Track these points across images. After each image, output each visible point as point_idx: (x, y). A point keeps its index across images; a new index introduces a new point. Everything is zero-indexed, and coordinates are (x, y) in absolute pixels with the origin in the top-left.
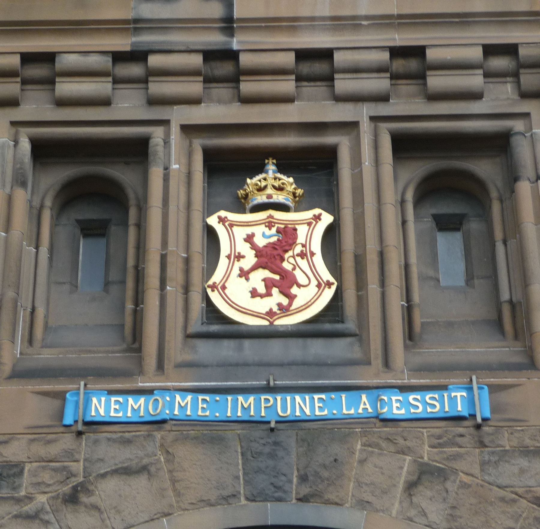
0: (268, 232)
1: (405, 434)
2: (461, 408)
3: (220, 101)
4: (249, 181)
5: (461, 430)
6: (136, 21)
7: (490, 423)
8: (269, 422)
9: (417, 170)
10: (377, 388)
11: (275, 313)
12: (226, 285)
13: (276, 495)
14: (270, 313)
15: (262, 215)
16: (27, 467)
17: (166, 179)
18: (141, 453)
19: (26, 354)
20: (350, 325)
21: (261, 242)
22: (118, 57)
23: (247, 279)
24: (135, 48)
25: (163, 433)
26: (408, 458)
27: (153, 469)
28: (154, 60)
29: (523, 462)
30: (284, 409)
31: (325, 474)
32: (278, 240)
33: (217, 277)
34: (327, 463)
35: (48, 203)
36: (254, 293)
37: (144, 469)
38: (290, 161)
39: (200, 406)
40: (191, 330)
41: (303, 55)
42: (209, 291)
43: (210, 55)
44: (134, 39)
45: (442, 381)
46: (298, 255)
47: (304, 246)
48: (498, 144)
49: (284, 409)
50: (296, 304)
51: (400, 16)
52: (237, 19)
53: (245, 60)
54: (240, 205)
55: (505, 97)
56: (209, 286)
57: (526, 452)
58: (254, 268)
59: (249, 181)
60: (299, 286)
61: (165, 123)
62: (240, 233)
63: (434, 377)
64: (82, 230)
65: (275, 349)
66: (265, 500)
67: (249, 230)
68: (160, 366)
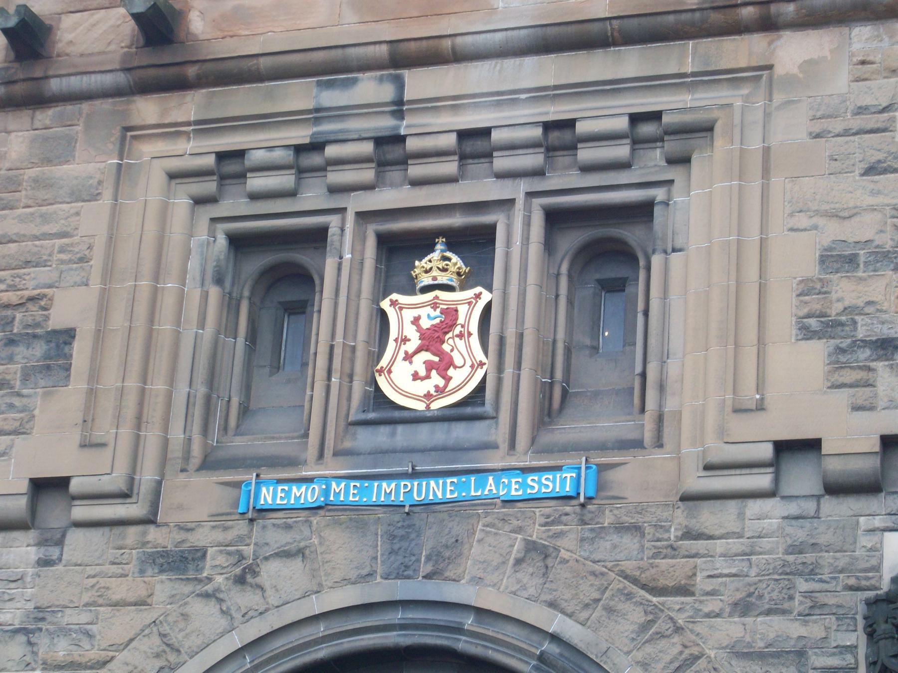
0: (434, 314)
1: (519, 515)
2: (568, 489)
3: (392, 185)
4: (417, 263)
5: (568, 509)
6: (317, 110)
7: (594, 501)
8: (404, 506)
9: (571, 240)
10: (503, 470)
11: (432, 395)
12: (392, 369)
13: (406, 573)
14: (428, 396)
15: (429, 296)
16: (210, 551)
17: (339, 269)
18: (298, 537)
19: (221, 443)
20: (488, 408)
21: (425, 324)
23: (411, 363)
24: (314, 140)
25: (318, 518)
26: (520, 536)
27: (307, 552)
28: (331, 151)
29: (615, 538)
30: (419, 493)
31: (447, 554)
32: (441, 322)
33: (384, 363)
34: (449, 543)
35: (246, 293)
36: (416, 376)
37: (300, 552)
38: (457, 240)
39: (352, 492)
40: (352, 418)
41: (464, 135)
42: (377, 375)
43: (380, 141)
44: (315, 129)
45: (559, 462)
46: (457, 336)
47: (463, 326)
49: (419, 493)
50: (452, 385)
51: (556, 87)
52: (408, 101)
53: (412, 144)
54: (410, 288)
55: (653, 164)
56: (377, 371)
57: (621, 528)
58: (417, 352)
59: (417, 263)
60: (455, 367)
61: (342, 211)
64: (286, 310)
65: (423, 435)
66: (396, 578)
67: (415, 313)
68: (321, 455)
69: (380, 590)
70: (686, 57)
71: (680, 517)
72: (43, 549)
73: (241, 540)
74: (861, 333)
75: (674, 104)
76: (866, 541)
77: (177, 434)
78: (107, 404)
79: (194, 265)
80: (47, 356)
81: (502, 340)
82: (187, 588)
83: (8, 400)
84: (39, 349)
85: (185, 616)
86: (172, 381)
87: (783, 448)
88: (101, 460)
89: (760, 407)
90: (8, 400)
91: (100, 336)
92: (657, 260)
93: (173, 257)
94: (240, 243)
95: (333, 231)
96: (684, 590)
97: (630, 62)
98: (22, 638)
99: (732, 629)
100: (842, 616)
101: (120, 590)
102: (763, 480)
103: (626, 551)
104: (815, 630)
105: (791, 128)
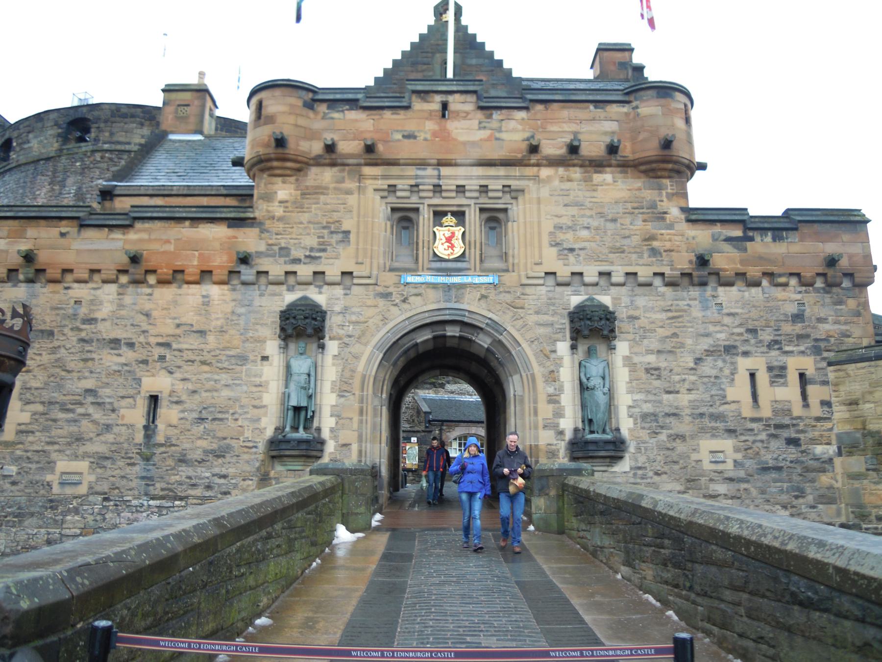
2: (491, 281)
20: (467, 259)
21: (447, 236)
22: (412, 186)
28: (421, 187)
38: (454, 214)
41: (457, 186)
43: (434, 186)
48: (505, 210)
53: (444, 188)
54: (441, 225)
61: (423, 204)
62: (442, 233)
63: (486, 271)
69: (442, 305)
70: (516, 171)
71: (519, 290)
73: (403, 290)
74: (565, 246)
75: (514, 184)
76: (567, 298)
79: (381, 215)
81: (470, 242)
84: (340, 236)
86: (379, 247)
87: (546, 273)
89: (541, 264)
91: (358, 233)
92: (510, 224)
94: (393, 210)
95: (421, 209)
96: (522, 308)
97: (502, 171)
99: (534, 318)
100: (562, 316)
101: (369, 303)
102: (541, 281)
103: (508, 298)
104: (555, 319)
105: (545, 192)
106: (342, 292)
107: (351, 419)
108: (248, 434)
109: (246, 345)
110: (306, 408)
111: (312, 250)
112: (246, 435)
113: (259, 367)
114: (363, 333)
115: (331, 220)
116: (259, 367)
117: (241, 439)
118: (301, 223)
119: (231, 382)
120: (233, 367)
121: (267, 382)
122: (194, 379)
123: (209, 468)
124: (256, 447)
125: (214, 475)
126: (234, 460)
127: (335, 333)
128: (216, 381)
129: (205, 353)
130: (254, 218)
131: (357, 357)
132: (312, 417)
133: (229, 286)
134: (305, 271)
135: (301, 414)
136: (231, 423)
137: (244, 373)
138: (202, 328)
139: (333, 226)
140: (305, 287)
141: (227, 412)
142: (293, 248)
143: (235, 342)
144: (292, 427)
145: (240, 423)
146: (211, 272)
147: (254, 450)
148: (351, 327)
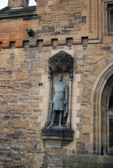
35: (110, 13)
72: (84, 47)
77: (104, 31)
78: (93, 27)
79: (103, 8)
80: (82, 20)
82: (109, 52)
83: (77, 26)
84: (81, 19)
85: (109, 56)
88: (93, 34)
90: (77, 26)
93: (100, 7)
98: (82, 60)
101: (98, 53)
106: (82, 48)
107: (89, 118)
108: (31, 126)
109: (31, 78)
110: (63, 112)
111: (65, 27)
112: (30, 126)
113: (38, 89)
114: (95, 69)
115: (75, 12)
116: (38, 89)
117: (27, 128)
118: (60, 15)
119: (22, 97)
120: (24, 89)
121: (42, 97)
122: (4, 96)
123: (10, 144)
124: (35, 133)
125: (12, 148)
126: (23, 140)
127: (79, 70)
128: (15, 96)
129: (11, 82)
130: (37, 15)
131: (92, 83)
132: (66, 117)
133: (24, 49)
134: (62, 38)
135: (59, 115)
136: (22, 119)
137: (29, 92)
138: (10, 70)
139: (76, 15)
140: (62, 46)
141: (20, 113)
142: (56, 27)
143: (26, 77)
144: (54, 122)
145: (27, 119)
146: (14, 42)
147: (34, 135)
148: (88, 66)
